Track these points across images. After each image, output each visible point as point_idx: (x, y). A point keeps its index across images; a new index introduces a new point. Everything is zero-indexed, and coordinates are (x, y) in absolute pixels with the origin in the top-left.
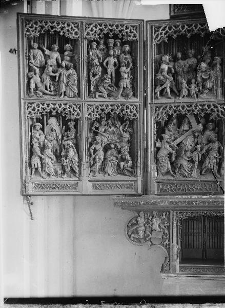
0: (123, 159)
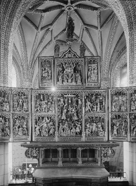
0: (24, 131)
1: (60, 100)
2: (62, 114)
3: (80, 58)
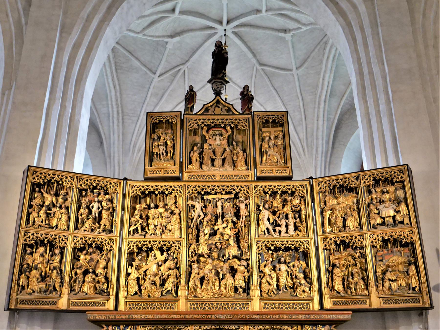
0: (99, 282)
1: (193, 206)
2: (198, 241)
3: (240, 114)
